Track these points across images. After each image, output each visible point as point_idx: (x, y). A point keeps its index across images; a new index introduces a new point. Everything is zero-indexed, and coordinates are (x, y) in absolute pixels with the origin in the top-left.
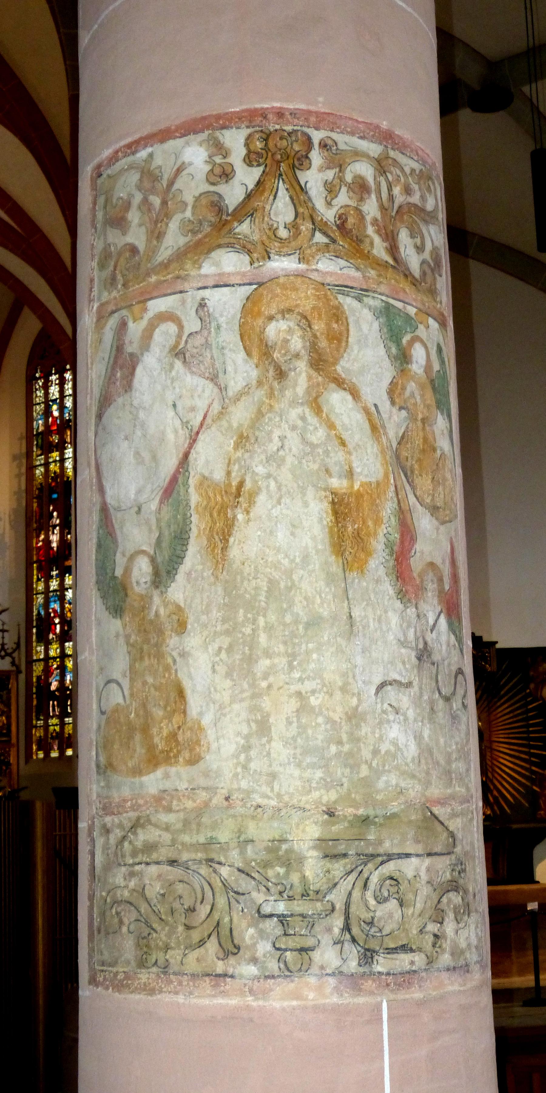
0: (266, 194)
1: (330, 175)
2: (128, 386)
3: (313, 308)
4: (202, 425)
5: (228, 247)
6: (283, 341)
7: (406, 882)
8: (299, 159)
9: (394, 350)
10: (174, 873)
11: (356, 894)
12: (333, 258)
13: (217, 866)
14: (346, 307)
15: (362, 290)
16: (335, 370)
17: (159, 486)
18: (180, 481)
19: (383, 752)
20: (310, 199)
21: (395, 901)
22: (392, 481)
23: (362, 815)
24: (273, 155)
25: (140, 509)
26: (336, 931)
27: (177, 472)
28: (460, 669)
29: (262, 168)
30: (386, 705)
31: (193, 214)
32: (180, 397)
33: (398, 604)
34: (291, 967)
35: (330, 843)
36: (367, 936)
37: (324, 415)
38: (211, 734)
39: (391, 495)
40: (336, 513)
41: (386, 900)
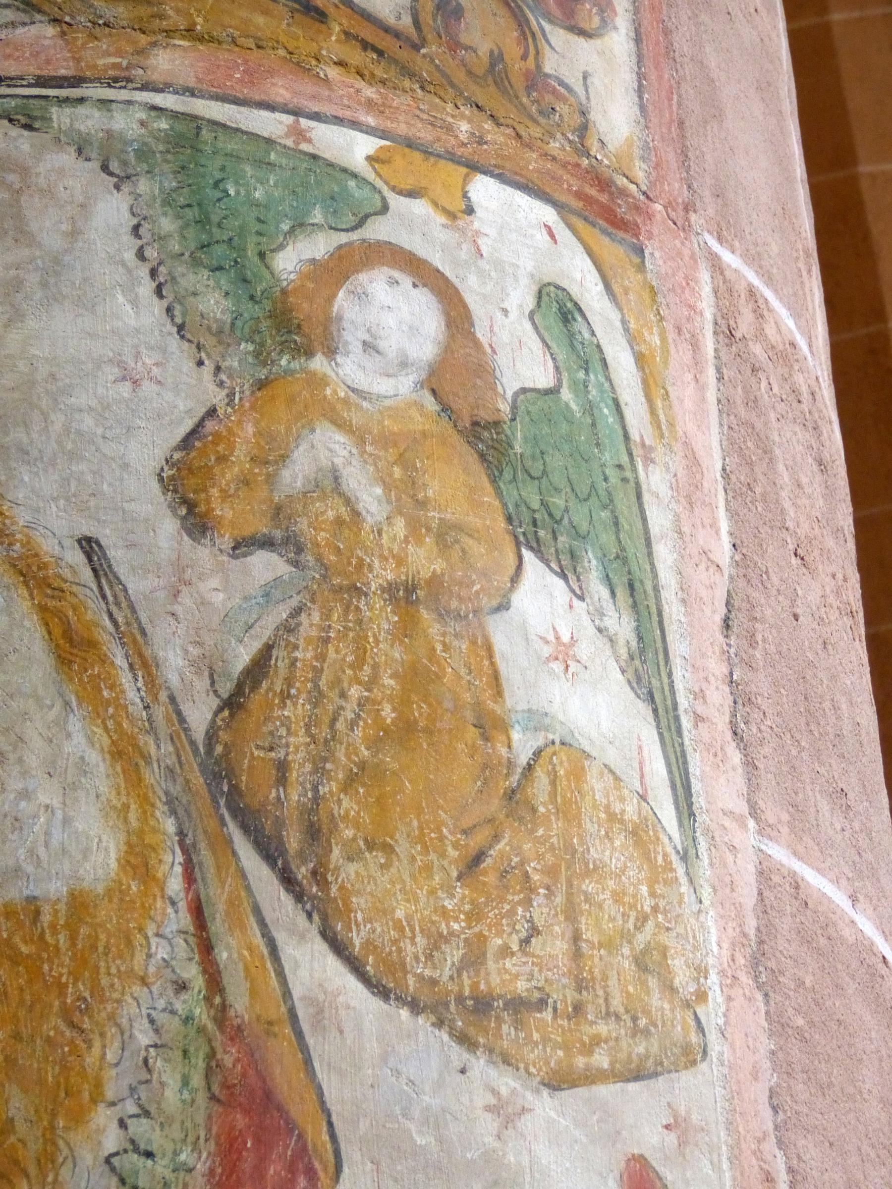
15: (42, 82)
22: (175, 885)
39: (161, 952)
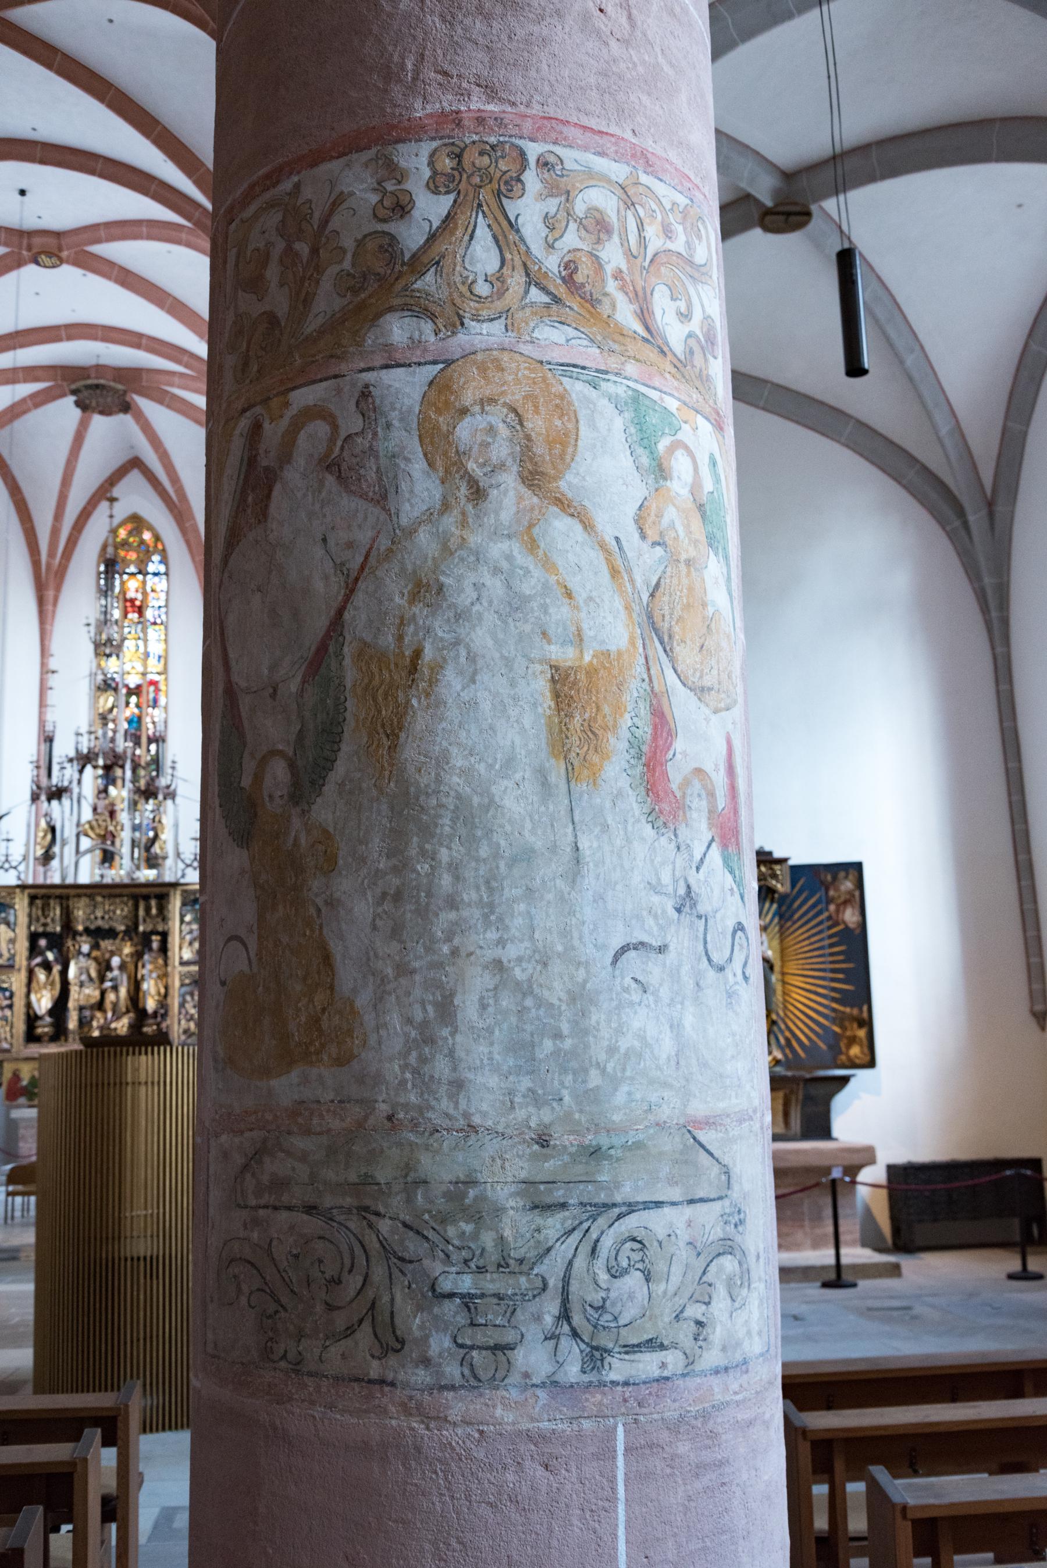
0: (459, 233)
1: (552, 205)
2: (263, 515)
3: (525, 397)
4: (362, 568)
5: (403, 310)
6: (481, 445)
7: (656, 1244)
8: (506, 183)
9: (645, 461)
10: (312, 1225)
11: (580, 1263)
12: (556, 324)
13: (373, 1218)
14: (574, 396)
15: (597, 371)
16: (558, 487)
17: (302, 657)
18: (331, 649)
19: (622, 1051)
20: (522, 239)
21: (638, 1272)
22: (641, 650)
23: (590, 1146)
24: (468, 177)
25: (275, 690)
26: (548, 1320)
27: (327, 636)
28: (739, 923)
29: (451, 197)
30: (628, 980)
31: (353, 265)
32: (333, 528)
33: (648, 831)
34: (481, 1373)
35: (542, 1187)
36: (595, 1327)
37: (541, 553)
38: (369, 1019)
40: (557, 695)
41: (625, 1272)
